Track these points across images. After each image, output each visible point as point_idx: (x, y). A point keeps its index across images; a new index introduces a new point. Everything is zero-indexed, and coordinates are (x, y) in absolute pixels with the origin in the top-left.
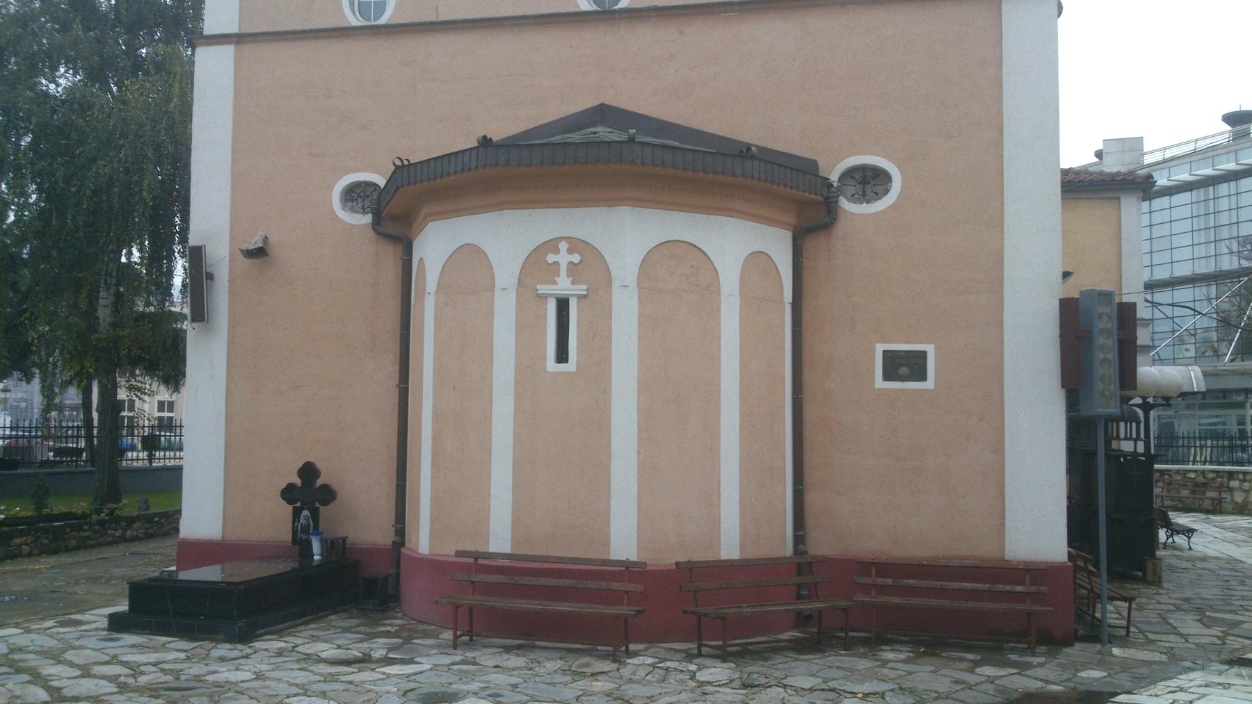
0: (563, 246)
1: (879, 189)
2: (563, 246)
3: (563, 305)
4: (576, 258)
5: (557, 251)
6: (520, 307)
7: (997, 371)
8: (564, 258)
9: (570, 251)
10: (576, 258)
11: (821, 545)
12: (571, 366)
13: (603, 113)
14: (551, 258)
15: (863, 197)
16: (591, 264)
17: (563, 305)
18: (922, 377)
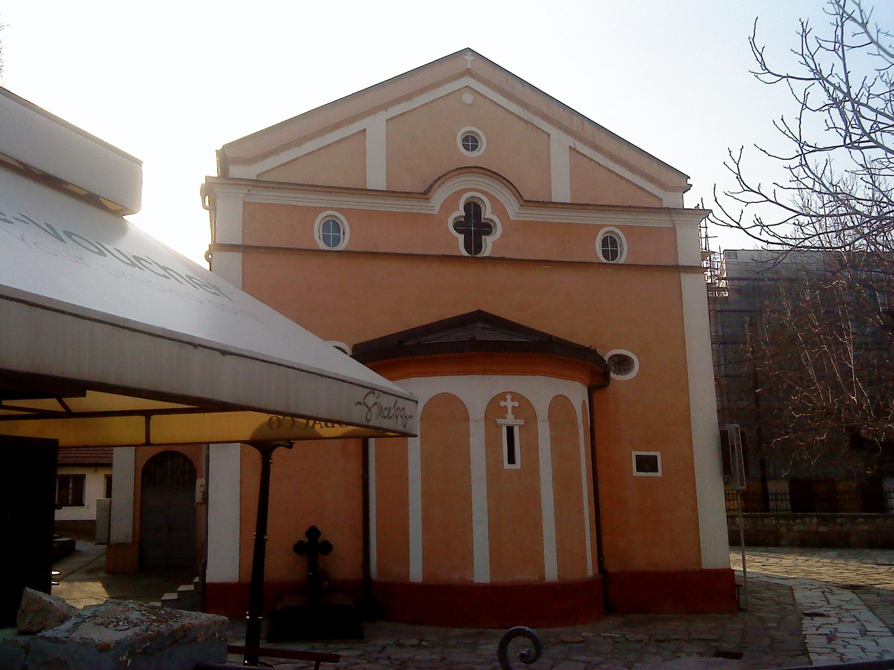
0: (509, 397)
1: (626, 367)
2: (509, 397)
3: (510, 430)
4: (516, 404)
5: (505, 400)
6: (487, 432)
7: (692, 468)
8: (509, 404)
9: (512, 400)
10: (516, 404)
11: (612, 567)
12: (517, 466)
13: (480, 316)
14: (502, 404)
15: (619, 372)
16: (524, 408)
17: (510, 430)
18: (656, 470)
